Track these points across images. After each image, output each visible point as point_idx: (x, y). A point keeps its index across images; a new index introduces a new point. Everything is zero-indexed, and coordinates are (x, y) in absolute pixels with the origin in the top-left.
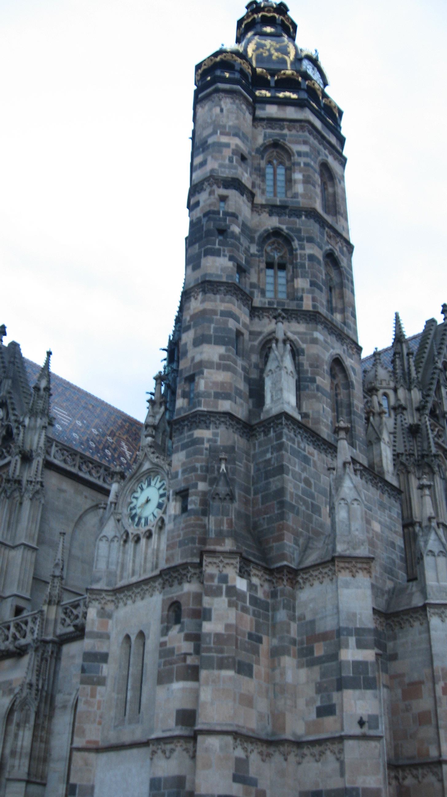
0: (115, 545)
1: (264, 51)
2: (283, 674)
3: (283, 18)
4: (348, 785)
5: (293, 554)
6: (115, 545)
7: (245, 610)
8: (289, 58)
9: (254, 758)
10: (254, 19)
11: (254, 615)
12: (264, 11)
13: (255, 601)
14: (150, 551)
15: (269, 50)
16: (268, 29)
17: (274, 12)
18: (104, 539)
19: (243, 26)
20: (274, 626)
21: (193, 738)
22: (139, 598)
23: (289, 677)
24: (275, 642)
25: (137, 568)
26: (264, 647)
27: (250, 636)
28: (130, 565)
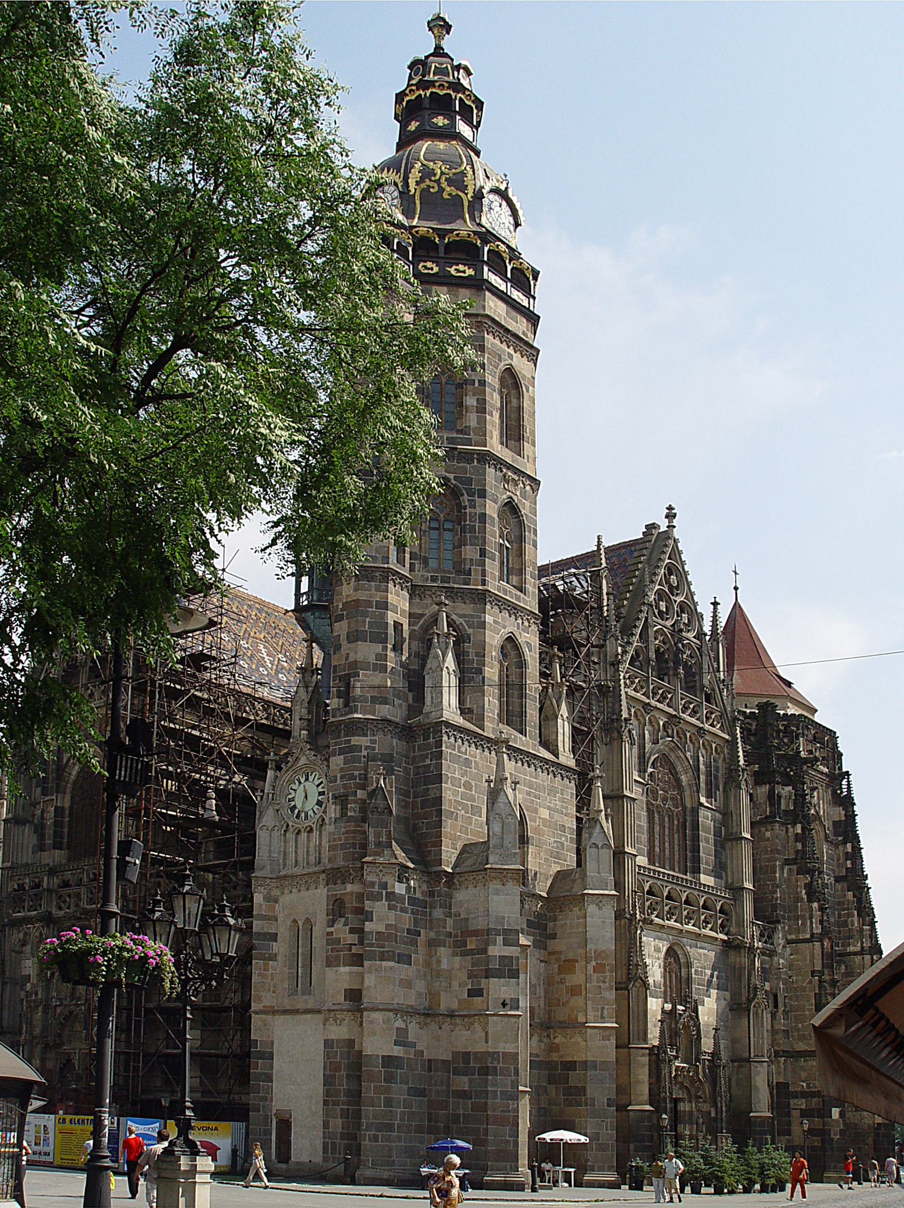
0: (276, 834)
1: (432, 184)
2: (439, 962)
3: (462, 96)
4: (490, 1050)
5: (451, 857)
6: (276, 834)
7: (403, 910)
8: (466, 194)
9: (413, 1027)
10: (420, 95)
11: (413, 913)
12: (435, 87)
13: (413, 901)
14: (312, 845)
15: (438, 182)
16: (440, 121)
17: (448, 88)
18: (265, 828)
19: (404, 104)
20: (431, 922)
21: (361, 1011)
22: (303, 888)
23: (444, 965)
24: (432, 935)
25: (300, 859)
26: (422, 939)
27: (409, 931)
28: (292, 856)
